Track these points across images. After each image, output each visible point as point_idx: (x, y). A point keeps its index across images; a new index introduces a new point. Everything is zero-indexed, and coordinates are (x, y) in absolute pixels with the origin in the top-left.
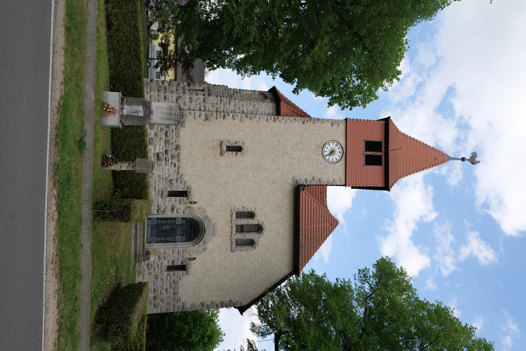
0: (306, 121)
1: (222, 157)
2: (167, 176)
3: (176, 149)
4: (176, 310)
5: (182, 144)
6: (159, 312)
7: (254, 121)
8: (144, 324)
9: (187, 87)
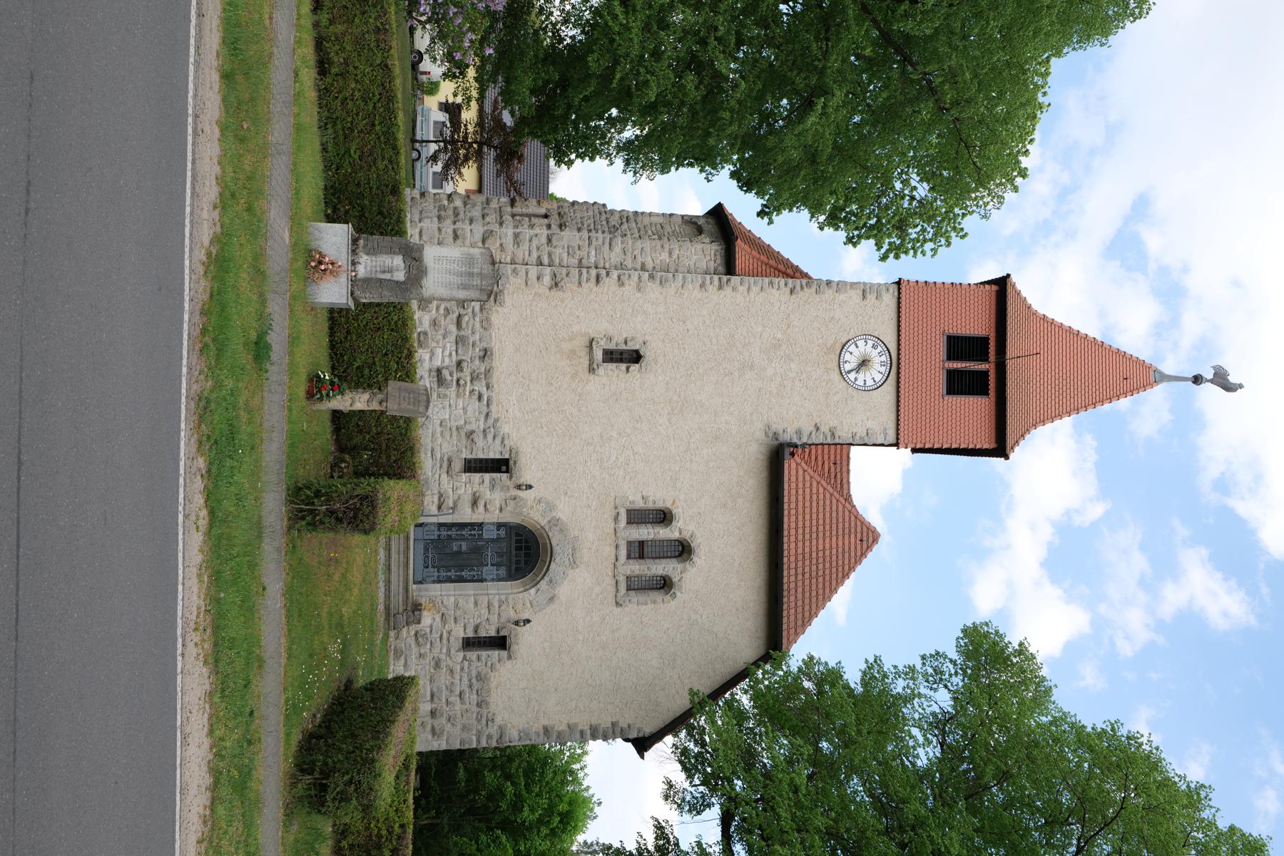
0: (798, 287)
1: (592, 377)
3: (483, 358)
4: (484, 744)
5: (496, 346)
6: (444, 747)
7: (671, 289)
8: (408, 776)
9: (509, 209)
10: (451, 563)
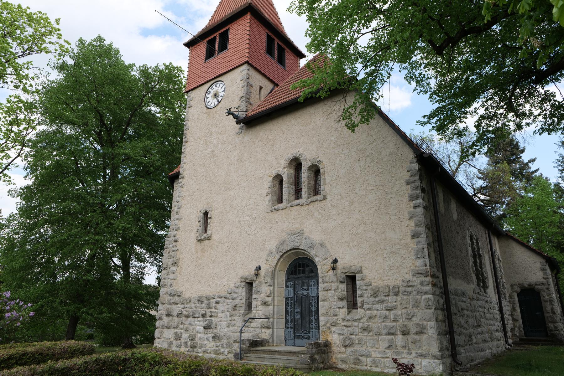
1: (213, 238)
2: (228, 313)
3: (202, 302)
4: (429, 288)
5: (196, 296)
6: (433, 323)
10: (307, 319)
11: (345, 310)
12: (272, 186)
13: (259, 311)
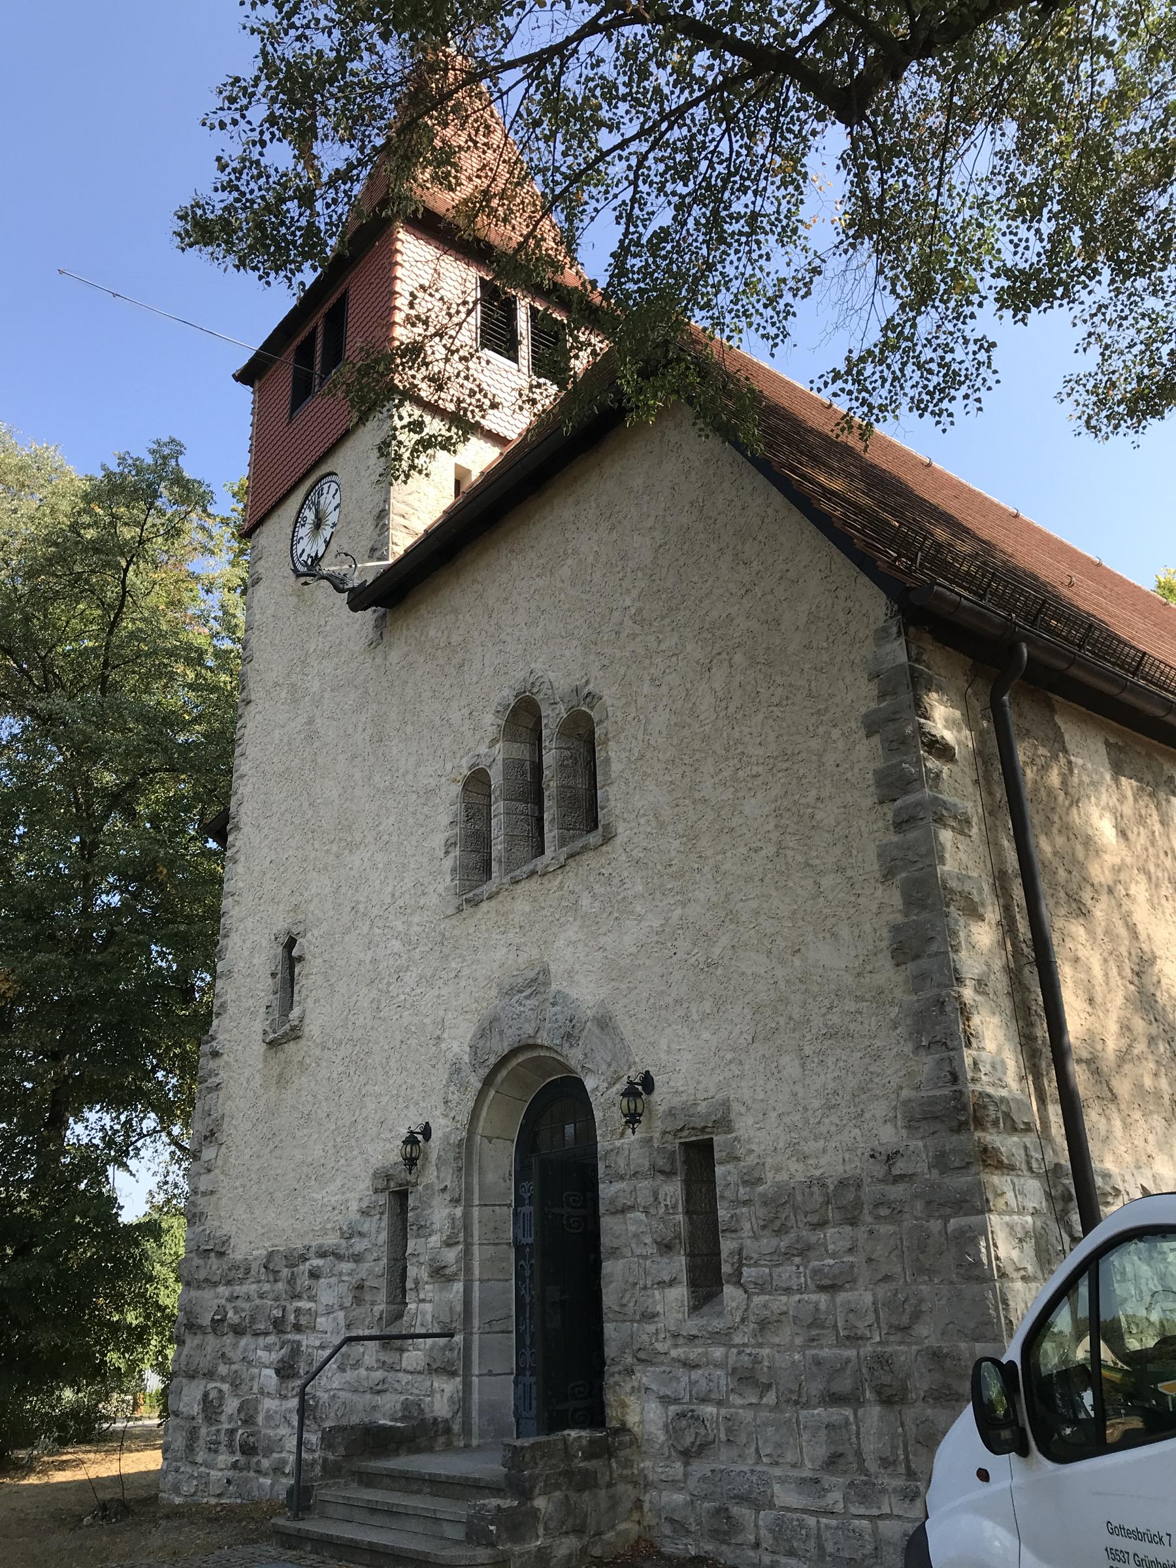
2: (341, 1314)
11: (680, 1293)
12: (462, 817)
13: (427, 1306)
